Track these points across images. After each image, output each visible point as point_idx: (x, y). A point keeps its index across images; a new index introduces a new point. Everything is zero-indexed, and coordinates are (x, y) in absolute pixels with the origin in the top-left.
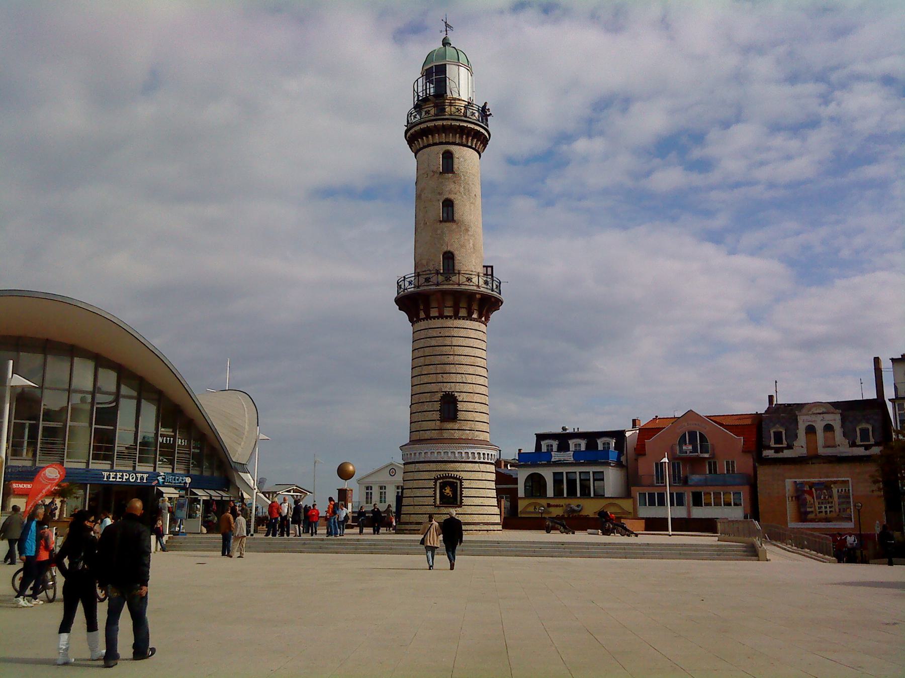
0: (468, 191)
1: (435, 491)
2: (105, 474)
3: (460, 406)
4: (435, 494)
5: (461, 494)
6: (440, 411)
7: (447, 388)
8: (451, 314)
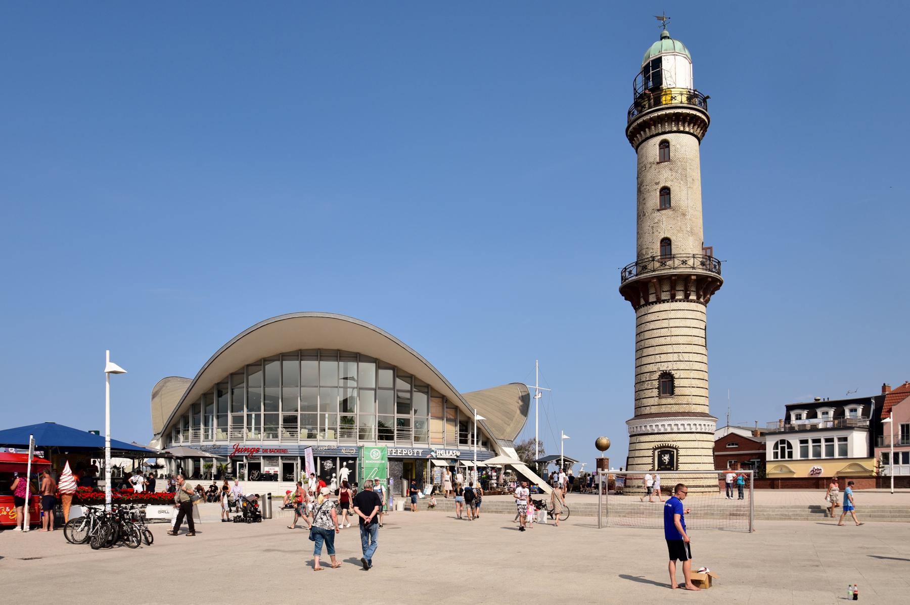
0: (684, 177)
1: (654, 459)
3: (677, 383)
4: (654, 461)
5: (677, 461)
6: (658, 388)
7: (664, 367)
8: (668, 297)
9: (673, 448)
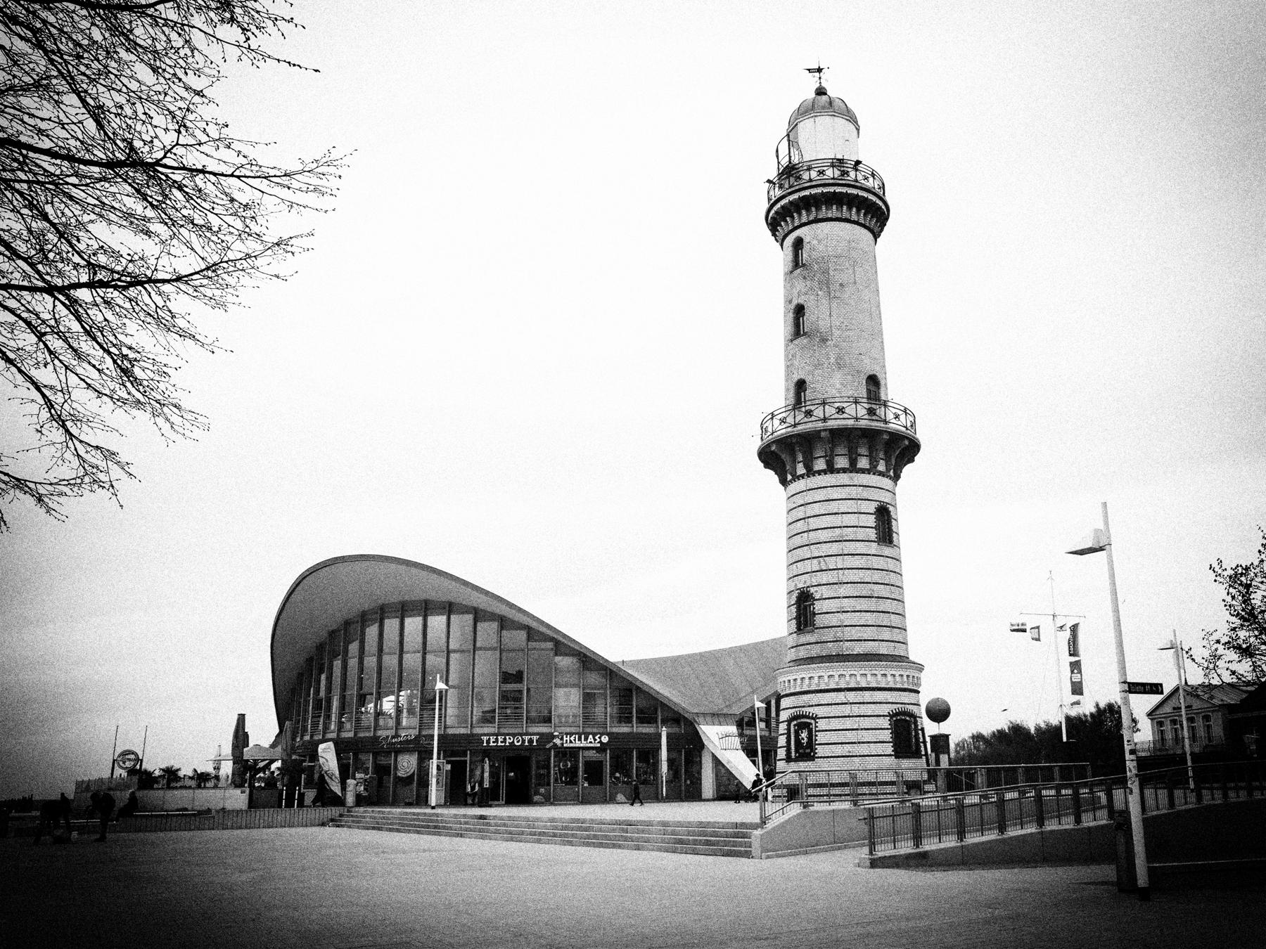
2: (485, 738)
3: (818, 607)
9: (808, 717)
